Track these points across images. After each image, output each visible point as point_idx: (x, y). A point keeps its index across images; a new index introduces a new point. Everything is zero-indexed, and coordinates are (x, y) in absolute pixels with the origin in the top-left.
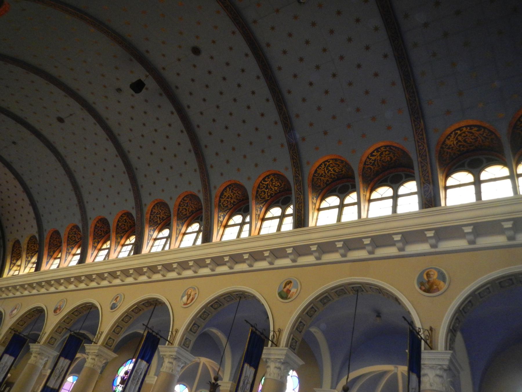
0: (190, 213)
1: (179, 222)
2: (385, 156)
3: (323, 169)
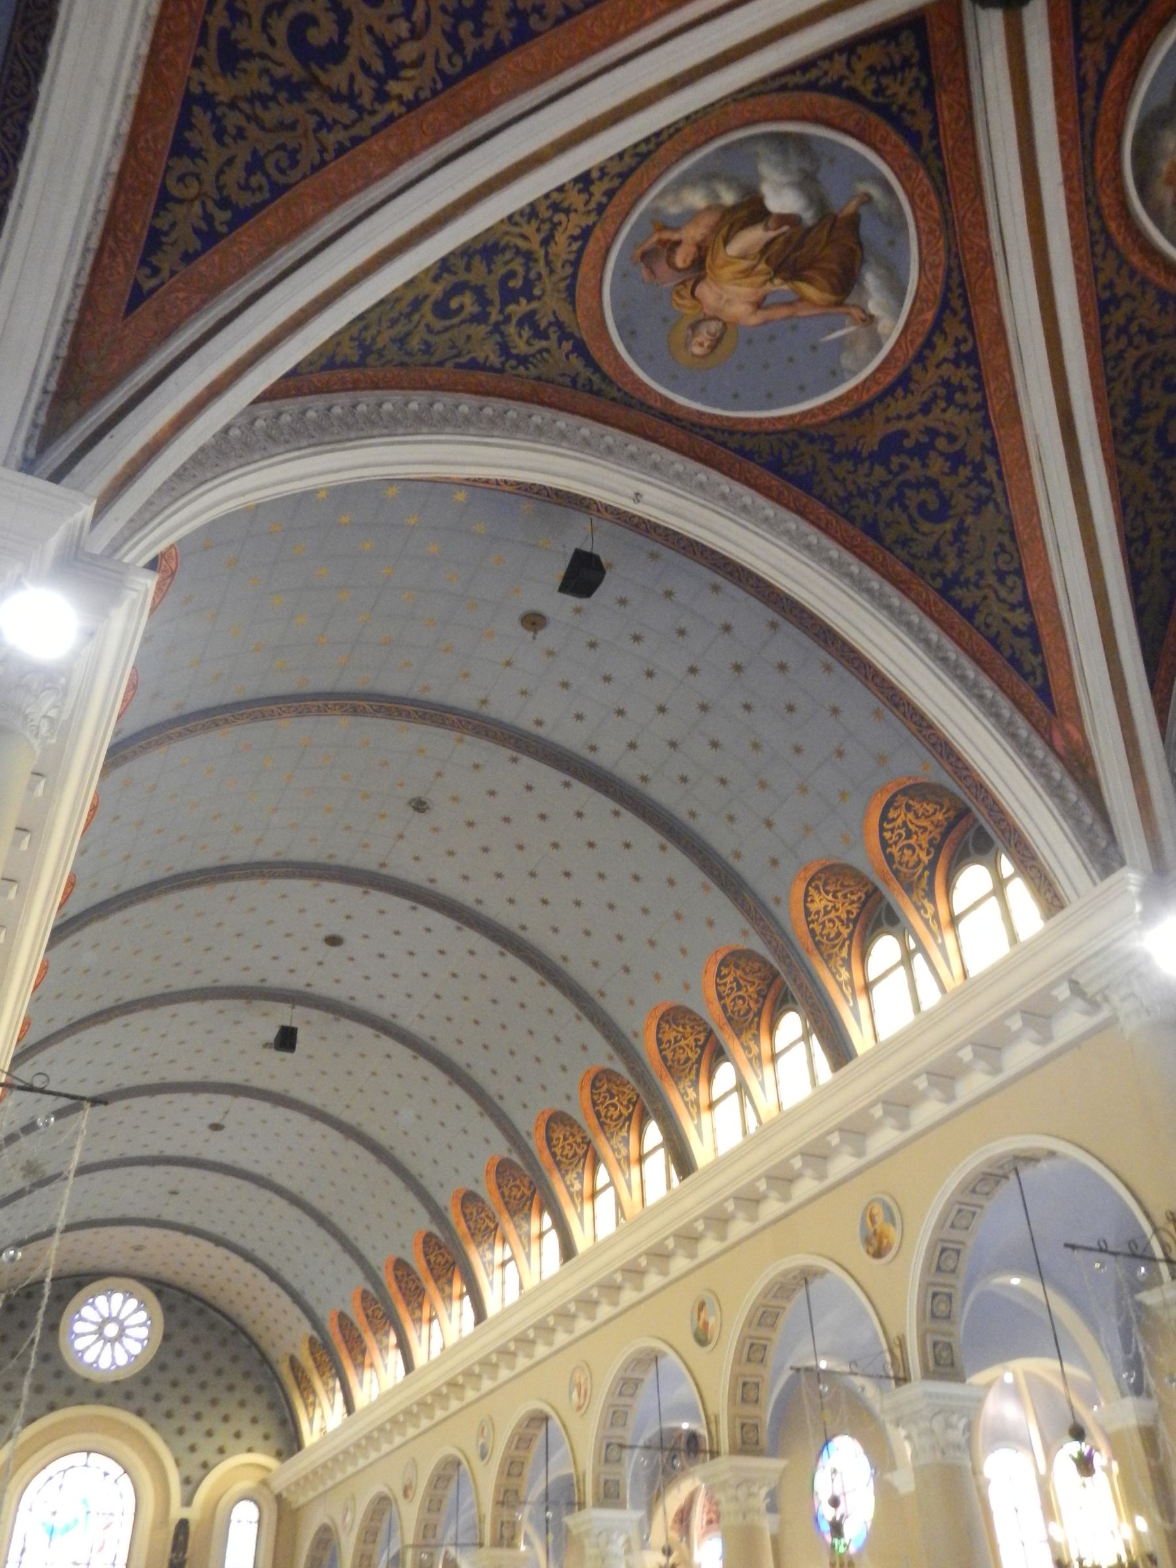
1: (516, 1218)
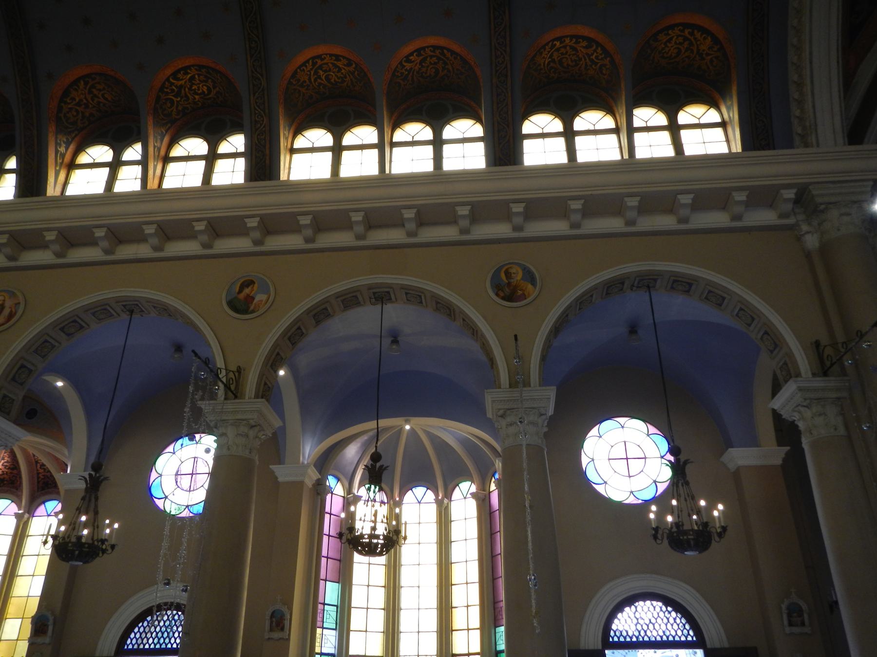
2: (428, 66)
3: (309, 73)
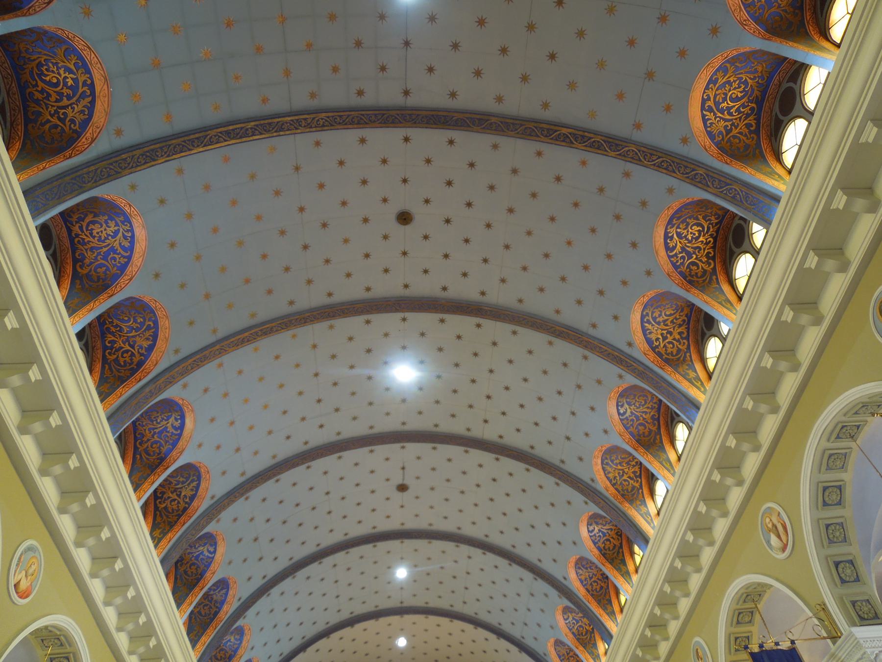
0: (654, 425)
3: (718, 119)
